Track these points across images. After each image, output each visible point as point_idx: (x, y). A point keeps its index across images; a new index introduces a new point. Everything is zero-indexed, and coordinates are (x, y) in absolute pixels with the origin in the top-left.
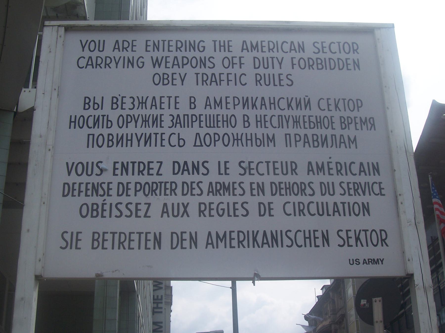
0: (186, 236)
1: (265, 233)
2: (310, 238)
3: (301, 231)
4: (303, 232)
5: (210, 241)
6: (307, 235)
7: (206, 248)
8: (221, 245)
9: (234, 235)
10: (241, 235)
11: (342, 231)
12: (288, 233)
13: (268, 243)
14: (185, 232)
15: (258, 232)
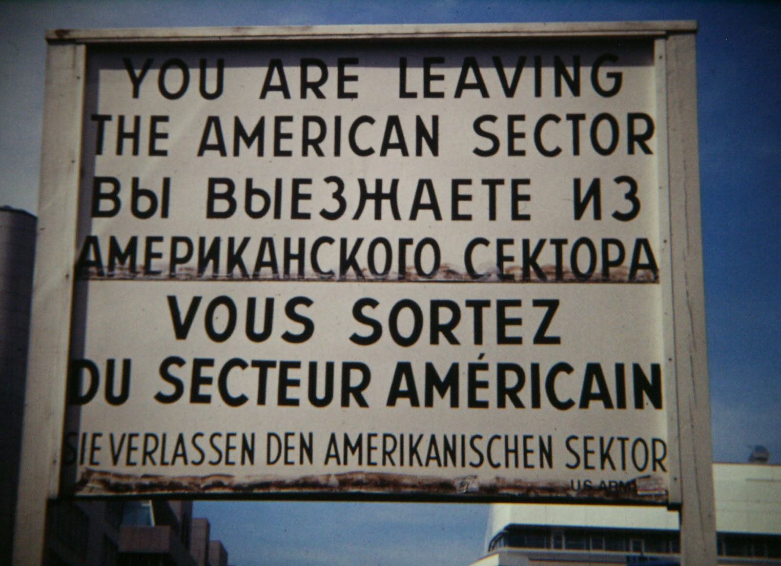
0: (294, 442)
1: (433, 441)
2: (515, 451)
3: (498, 437)
4: (503, 439)
5: (333, 452)
6: (511, 446)
7: (326, 462)
8: (353, 459)
9: (377, 442)
10: (390, 441)
11: (576, 438)
12: (477, 442)
13: (437, 458)
14: (293, 434)
15: (421, 437)
